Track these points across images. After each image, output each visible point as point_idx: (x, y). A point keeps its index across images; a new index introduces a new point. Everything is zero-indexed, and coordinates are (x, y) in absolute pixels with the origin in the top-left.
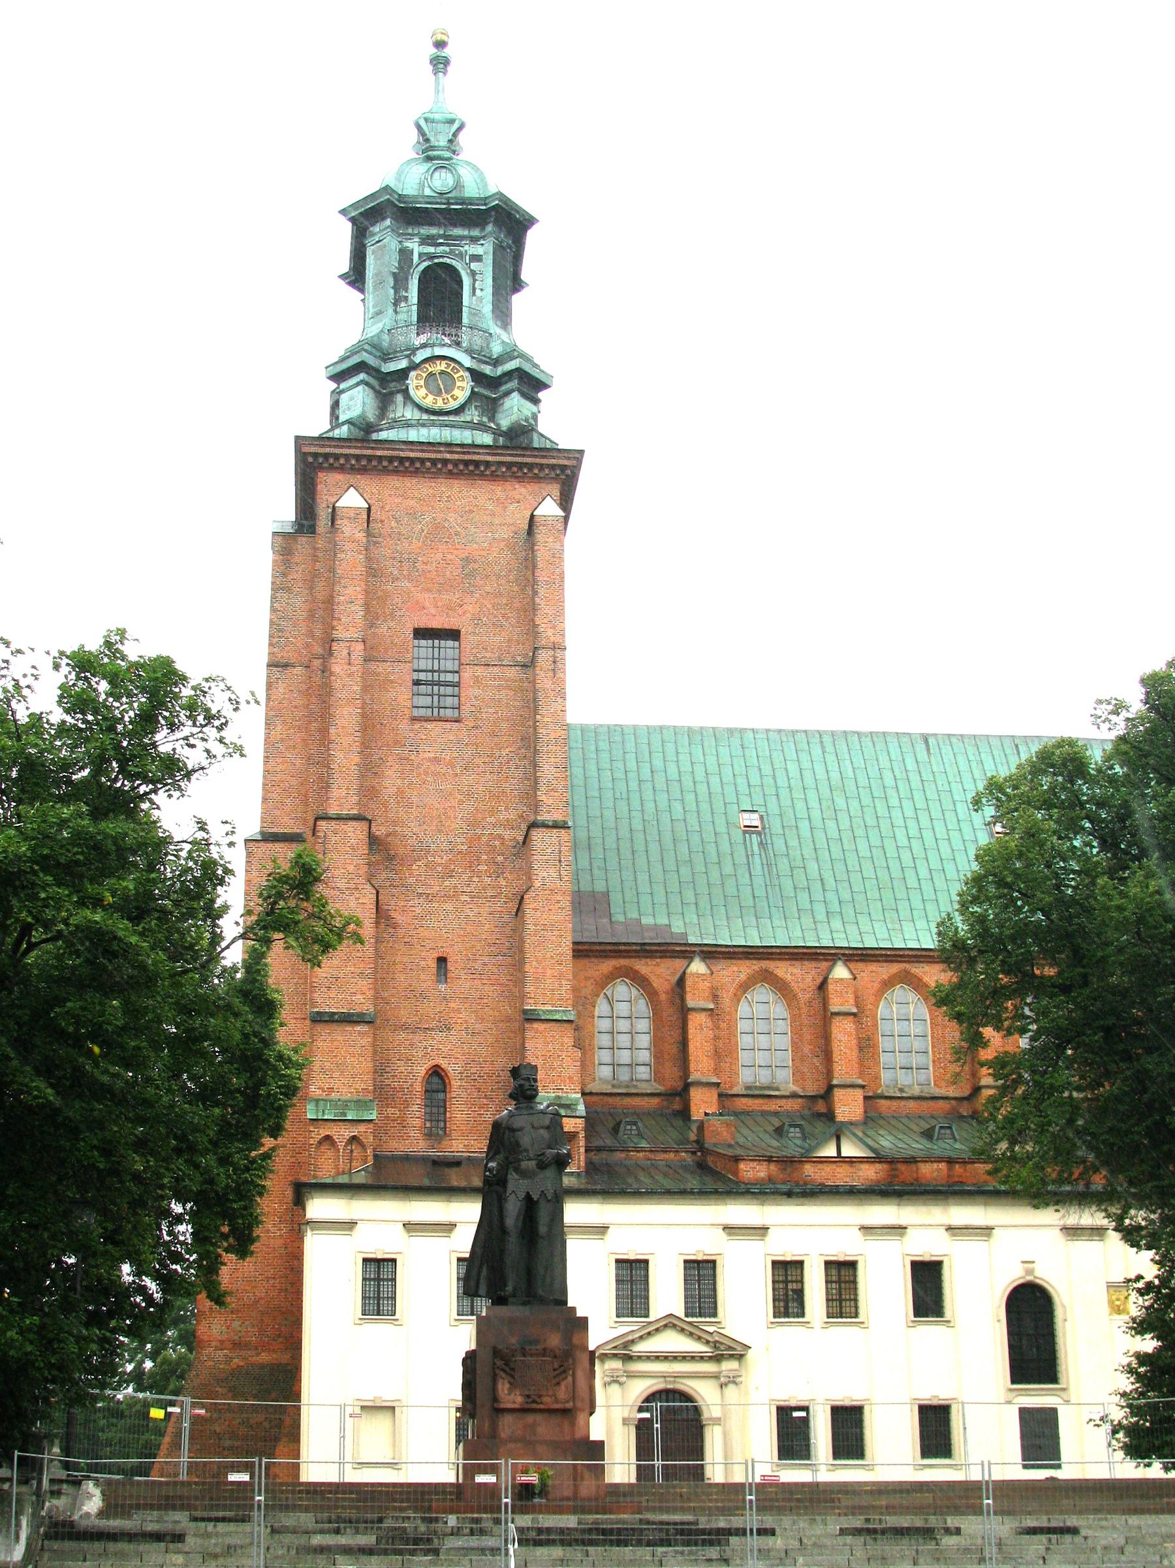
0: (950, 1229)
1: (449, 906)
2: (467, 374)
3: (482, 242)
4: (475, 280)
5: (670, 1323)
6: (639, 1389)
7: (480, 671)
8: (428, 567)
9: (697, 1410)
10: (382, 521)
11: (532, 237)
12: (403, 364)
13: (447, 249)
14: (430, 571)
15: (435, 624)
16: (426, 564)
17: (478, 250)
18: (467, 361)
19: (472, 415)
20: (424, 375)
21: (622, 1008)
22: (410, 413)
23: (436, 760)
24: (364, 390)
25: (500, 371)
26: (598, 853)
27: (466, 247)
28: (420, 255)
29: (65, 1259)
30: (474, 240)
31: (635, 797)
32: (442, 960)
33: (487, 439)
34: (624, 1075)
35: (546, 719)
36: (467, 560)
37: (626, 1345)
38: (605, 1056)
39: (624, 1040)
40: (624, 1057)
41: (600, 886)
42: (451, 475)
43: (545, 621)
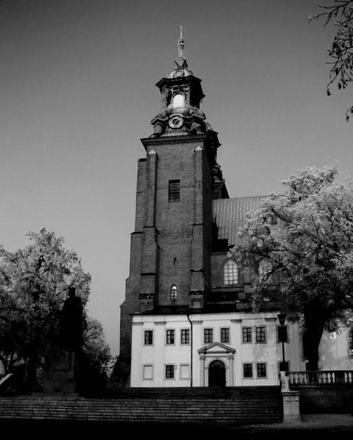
0: (266, 319)
1: (177, 246)
5: (216, 344)
6: (208, 361)
7: (185, 189)
9: (224, 365)
11: (201, 83)
15: (174, 179)
17: (187, 89)
19: (184, 128)
21: (231, 267)
22: (170, 129)
23: (174, 211)
26: (226, 230)
29: (18, 333)
30: (186, 87)
31: (238, 216)
32: (175, 259)
33: (186, 134)
34: (231, 283)
36: (181, 163)
37: (205, 350)
38: (226, 279)
39: (231, 275)
40: (231, 279)
41: (226, 238)
42: (178, 143)
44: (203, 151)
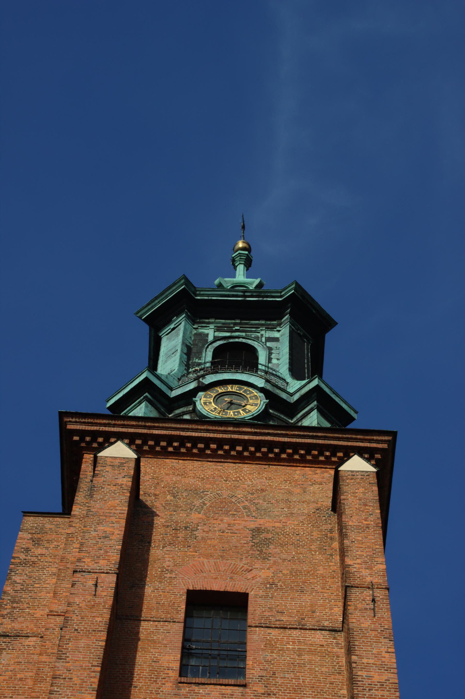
2: (262, 395)
3: (278, 329)
4: (270, 354)
8: (210, 535)
10: (155, 495)
11: (329, 337)
12: (192, 386)
13: (244, 334)
14: (211, 539)
16: (207, 532)
18: (260, 383)
20: (214, 395)
24: (146, 407)
25: (296, 397)
27: (263, 332)
28: (214, 337)
35: (365, 661)
36: (258, 531)
43: (359, 561)
44: (377, 473)
